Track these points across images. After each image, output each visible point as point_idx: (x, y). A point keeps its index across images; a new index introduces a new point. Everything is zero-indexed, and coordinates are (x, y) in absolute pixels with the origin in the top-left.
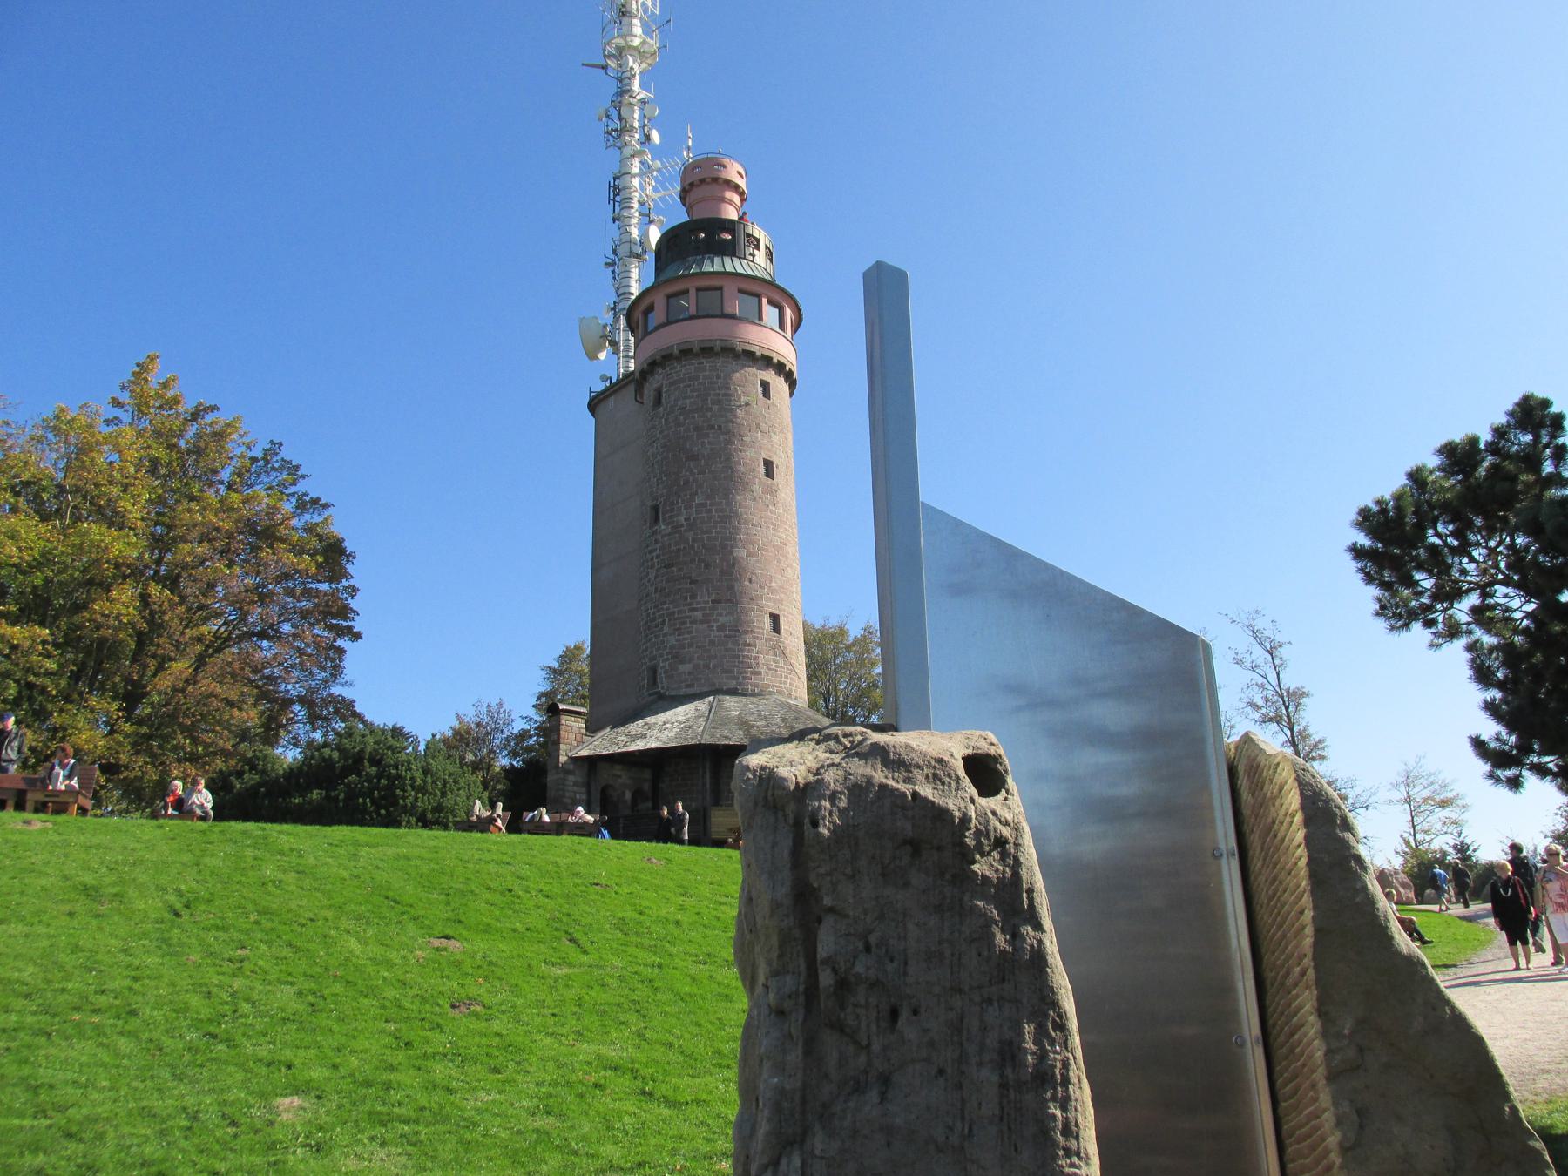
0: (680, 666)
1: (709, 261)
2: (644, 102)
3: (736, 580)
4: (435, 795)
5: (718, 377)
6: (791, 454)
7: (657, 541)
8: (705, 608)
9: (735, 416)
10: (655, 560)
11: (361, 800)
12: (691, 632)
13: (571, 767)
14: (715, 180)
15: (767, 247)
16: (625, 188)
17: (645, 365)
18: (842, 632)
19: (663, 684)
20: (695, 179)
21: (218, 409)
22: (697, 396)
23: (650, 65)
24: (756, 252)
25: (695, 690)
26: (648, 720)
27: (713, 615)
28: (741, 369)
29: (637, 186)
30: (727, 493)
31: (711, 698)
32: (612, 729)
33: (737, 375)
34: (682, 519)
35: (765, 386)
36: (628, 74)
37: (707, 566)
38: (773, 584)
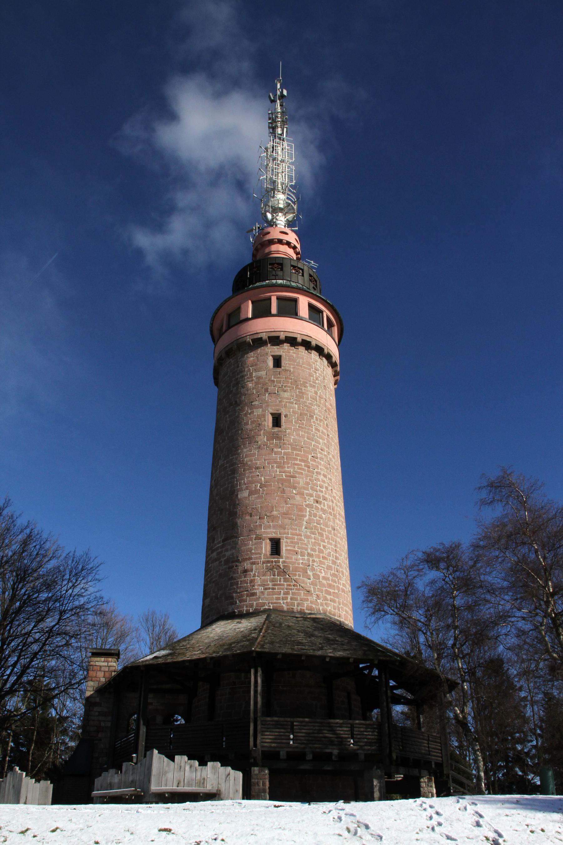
38: (275, 513)
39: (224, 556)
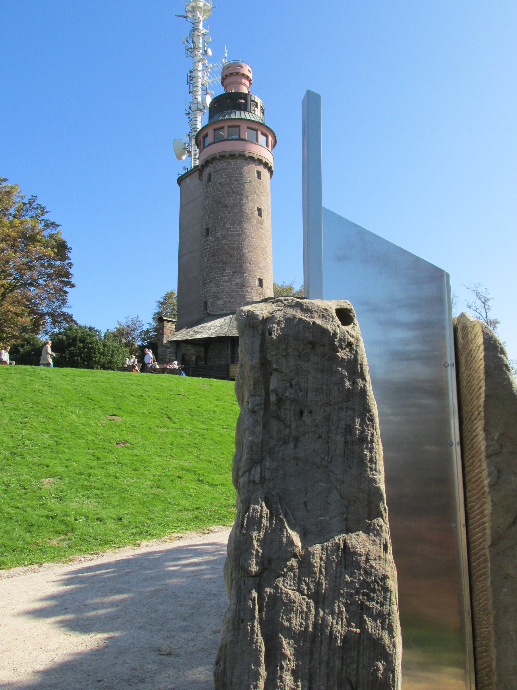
0: (218, 301)
1: (234, 113)
2: (204, 34)
3: (243, 263)
4: (109, 356)
5: (237, 168)
6: (270, 205)
7: (208, 245)
8: (228, 276)
9: (245, 187)
10: (207, 253)
11: (76, 358)
12: (223, 286)
13: (169, 345)
14: (238, 74)
15: (261, 107)
16: (195, 77)
17: (204, 163)
18: (291, 288)
19: (210, 309)
20: (228, 73)
21: (7, 180)
22: (228, 177)
23: (208, 16)
24: (256, 109)
25: (225, 312)
26: (203, 325)
27: (233, 278)
28: (248, 165)
29: (201, 76)
30: (240, 223)
31: (231, 316)
32: (186, 329)
33: (246, 167)
35: (259, 173)
36: (197, 21)
37: (231, 256)
38: (260, 265)
39: (234, 281)
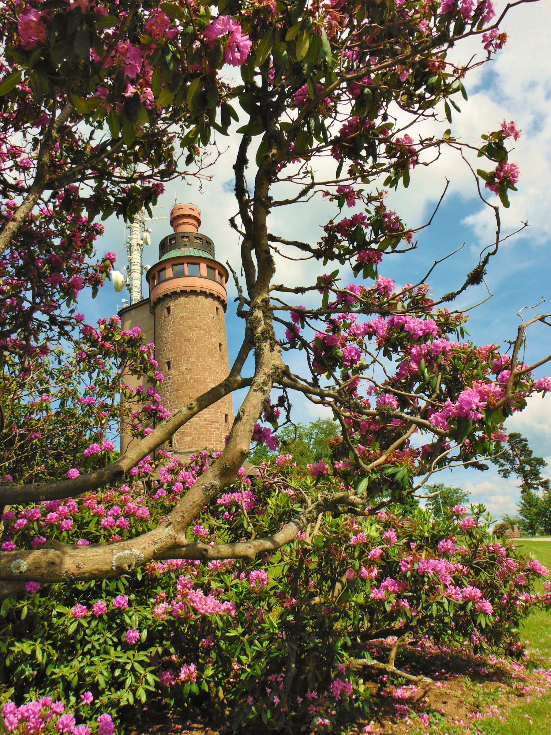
5: (199, 304)
7: (169, 379)
34: (184, 368)
39: (203, 417)
